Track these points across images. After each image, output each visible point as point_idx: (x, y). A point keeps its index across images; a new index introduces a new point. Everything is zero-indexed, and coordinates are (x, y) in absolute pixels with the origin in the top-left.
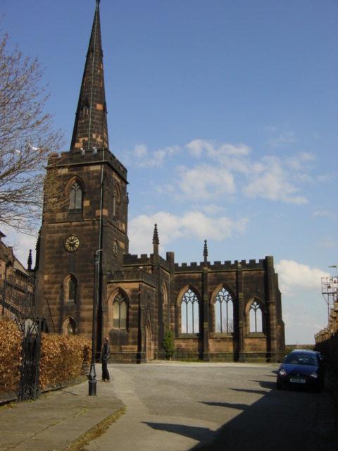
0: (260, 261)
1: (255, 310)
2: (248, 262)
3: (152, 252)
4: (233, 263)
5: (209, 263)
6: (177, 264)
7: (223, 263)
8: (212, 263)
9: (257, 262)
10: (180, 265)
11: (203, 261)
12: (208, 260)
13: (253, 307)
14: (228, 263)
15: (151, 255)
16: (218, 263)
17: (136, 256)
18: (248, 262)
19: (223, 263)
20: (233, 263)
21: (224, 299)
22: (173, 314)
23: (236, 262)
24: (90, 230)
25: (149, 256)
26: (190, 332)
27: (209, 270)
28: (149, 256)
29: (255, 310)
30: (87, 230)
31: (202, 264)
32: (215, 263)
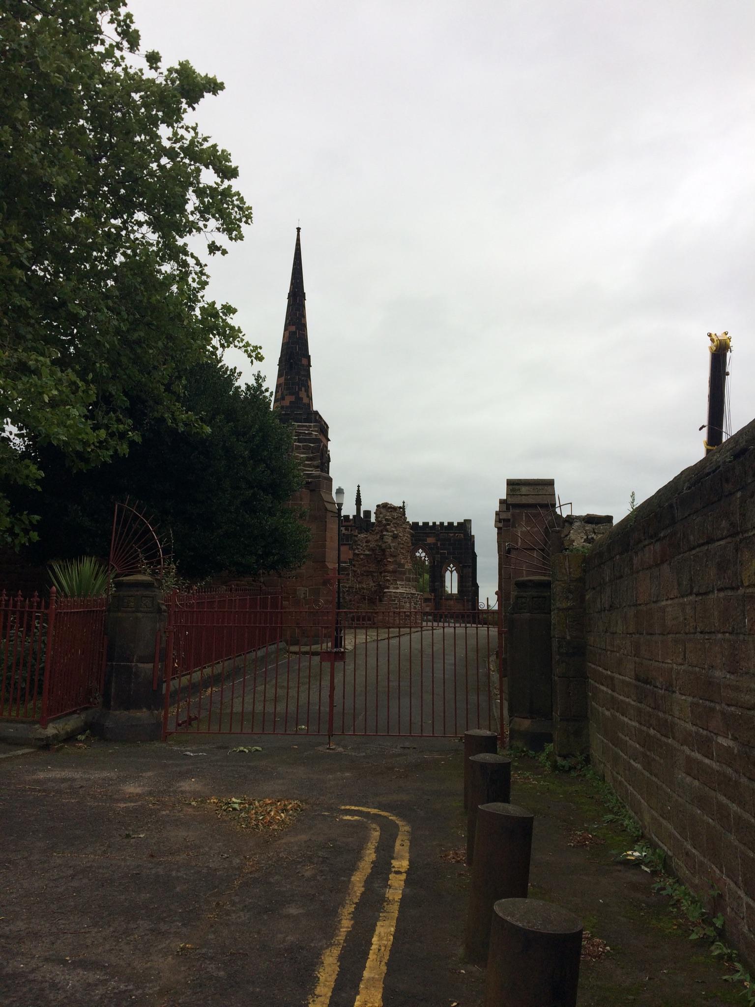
1: (451, 572)
2: (446, 524)
3: (355, 514)
4: (431, 524)
9: (455, 524)
13: (450, 569)
14: (426, 524)
16: (416, 524)
18: (446, 524)
20: (431, 524)
23: (434, 523)
25: (351, 517)
28: (351, 517)
29: (451, 572)
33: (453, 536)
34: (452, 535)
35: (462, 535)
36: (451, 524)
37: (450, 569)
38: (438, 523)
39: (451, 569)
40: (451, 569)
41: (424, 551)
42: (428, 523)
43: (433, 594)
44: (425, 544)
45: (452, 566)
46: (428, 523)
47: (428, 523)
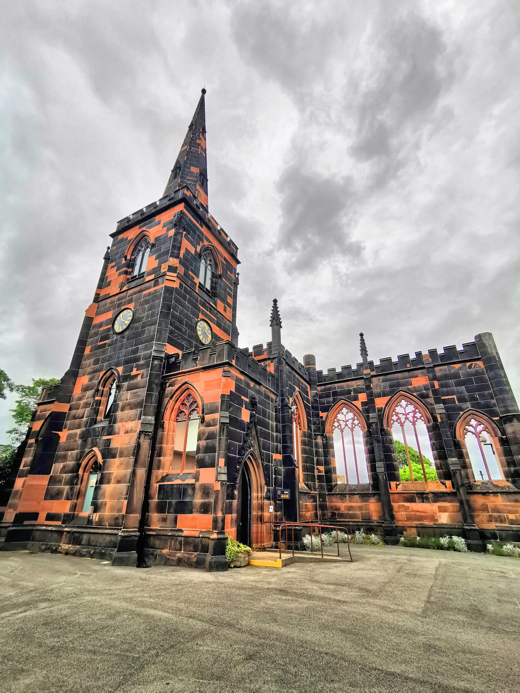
0: (465, 346)
3: (270, 340)
4: (412, 356)
5: (371, 363)
6: (321, 372)
7: (395, 359)
8: (377, 363)
10: (325, 373)
11: (361, 360)
12: (369, 359)
13: (470, 428)
15: (269, 344)
17: (247, 350)
19: (395, 359)
20: (412, 356)
21: (407, 418)
22: (321, 450)
24: (149, 294)
25: (265, 347)
26: (353, 482)
27: (374, 373)
28: (265, 347)
30: (145, 296)
31: (360, 366)
32: (382, 361)
33: (460, 369)
34: (459, 365)
35: (480, 363)
36: (450, 350)
37: (470, 428)
38: (425, 352)
39: (475, 428)
40: (475, 428)
41: (410, 401)
42: (407, 356)
43: (448, 483)
44: (409, 389)
45: (473, 422)
46: (407, 356)
47: (407, 356)
